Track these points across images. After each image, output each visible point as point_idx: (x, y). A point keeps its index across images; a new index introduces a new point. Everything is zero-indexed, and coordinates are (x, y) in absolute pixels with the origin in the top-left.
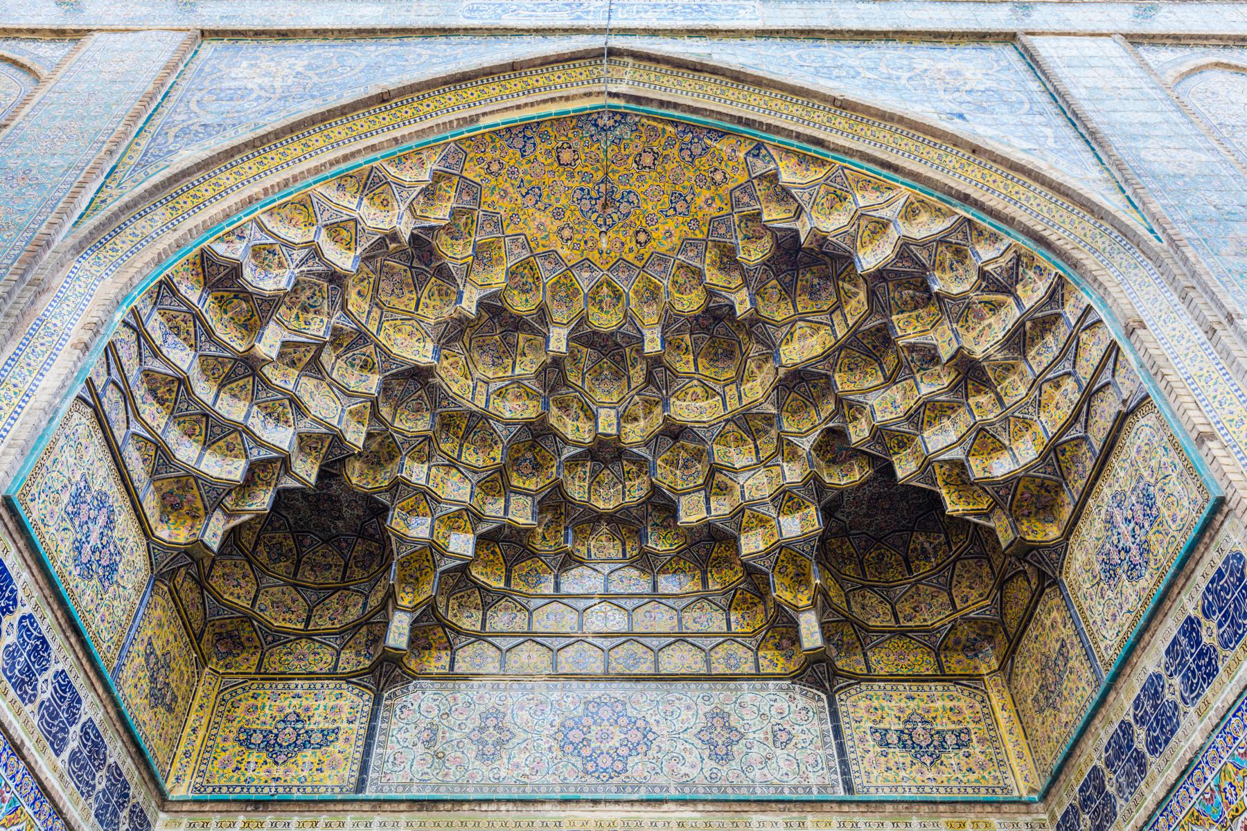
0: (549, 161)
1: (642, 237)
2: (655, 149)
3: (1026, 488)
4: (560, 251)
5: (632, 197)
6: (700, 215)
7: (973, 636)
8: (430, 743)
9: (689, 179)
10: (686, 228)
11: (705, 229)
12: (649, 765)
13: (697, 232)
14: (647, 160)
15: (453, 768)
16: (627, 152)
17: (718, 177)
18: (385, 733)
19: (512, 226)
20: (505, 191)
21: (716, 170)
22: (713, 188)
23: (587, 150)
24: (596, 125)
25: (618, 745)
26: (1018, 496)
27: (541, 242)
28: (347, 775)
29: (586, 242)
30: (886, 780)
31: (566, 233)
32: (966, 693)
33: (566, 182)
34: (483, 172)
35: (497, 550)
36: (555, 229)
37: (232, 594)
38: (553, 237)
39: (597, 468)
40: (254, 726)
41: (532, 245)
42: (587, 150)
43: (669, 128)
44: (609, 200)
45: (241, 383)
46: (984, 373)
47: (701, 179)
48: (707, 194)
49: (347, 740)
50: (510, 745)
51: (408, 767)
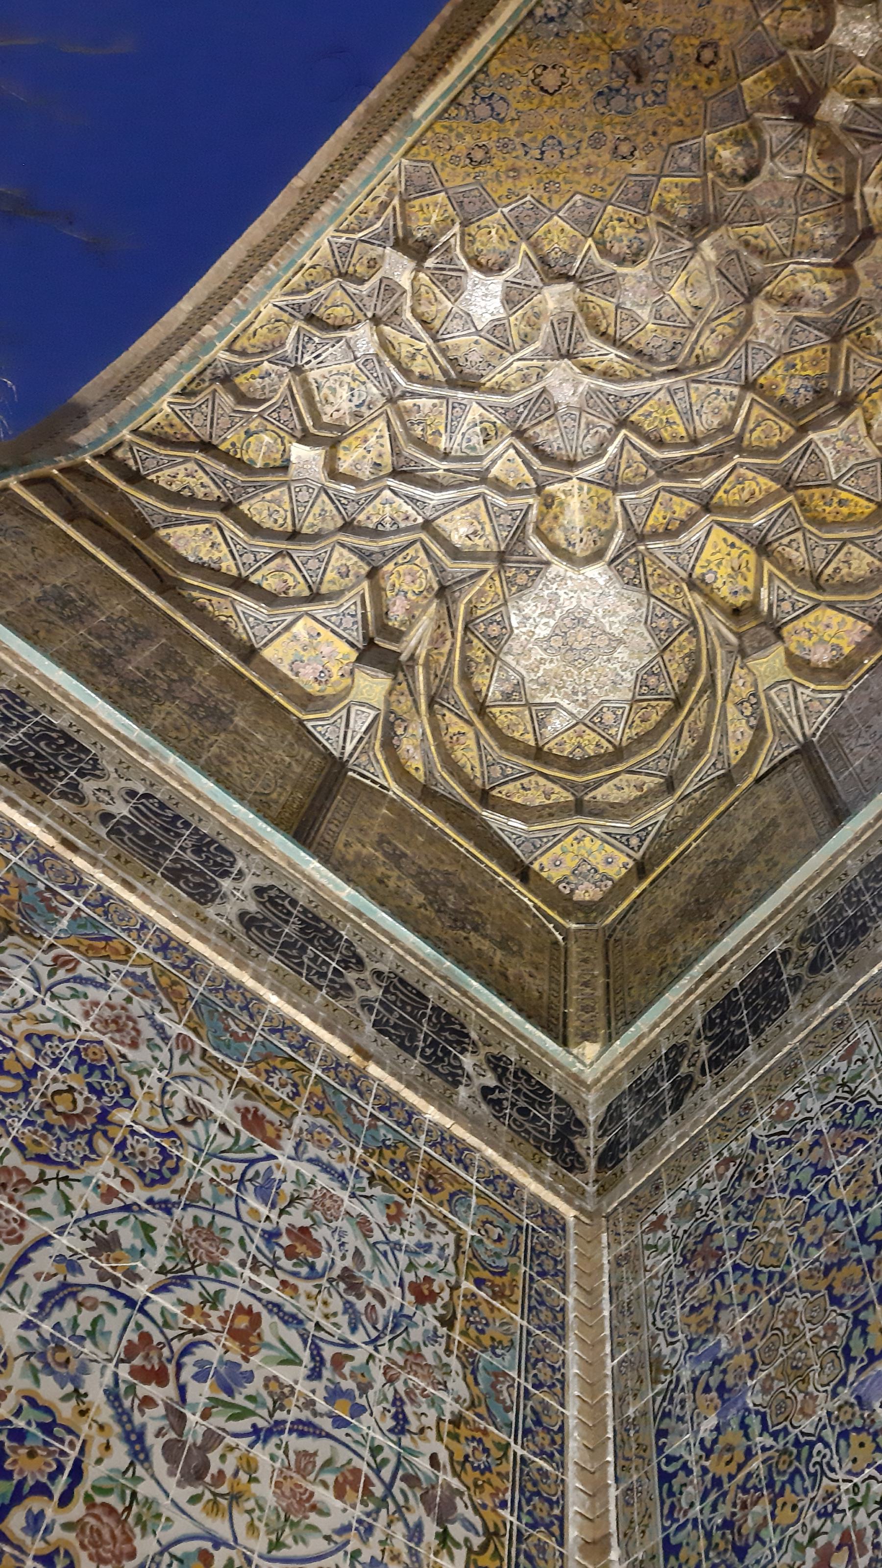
0: (536, 101)
4: (634, 170)
19: (555, 198)
20: (514, 169)
27: (604, 185)
31: (624, 149)
33: (576, 105)
34: (469, 169)
36: (607, 157)
38: (614, 166)
41: (597, 194)
45: (316, 510)
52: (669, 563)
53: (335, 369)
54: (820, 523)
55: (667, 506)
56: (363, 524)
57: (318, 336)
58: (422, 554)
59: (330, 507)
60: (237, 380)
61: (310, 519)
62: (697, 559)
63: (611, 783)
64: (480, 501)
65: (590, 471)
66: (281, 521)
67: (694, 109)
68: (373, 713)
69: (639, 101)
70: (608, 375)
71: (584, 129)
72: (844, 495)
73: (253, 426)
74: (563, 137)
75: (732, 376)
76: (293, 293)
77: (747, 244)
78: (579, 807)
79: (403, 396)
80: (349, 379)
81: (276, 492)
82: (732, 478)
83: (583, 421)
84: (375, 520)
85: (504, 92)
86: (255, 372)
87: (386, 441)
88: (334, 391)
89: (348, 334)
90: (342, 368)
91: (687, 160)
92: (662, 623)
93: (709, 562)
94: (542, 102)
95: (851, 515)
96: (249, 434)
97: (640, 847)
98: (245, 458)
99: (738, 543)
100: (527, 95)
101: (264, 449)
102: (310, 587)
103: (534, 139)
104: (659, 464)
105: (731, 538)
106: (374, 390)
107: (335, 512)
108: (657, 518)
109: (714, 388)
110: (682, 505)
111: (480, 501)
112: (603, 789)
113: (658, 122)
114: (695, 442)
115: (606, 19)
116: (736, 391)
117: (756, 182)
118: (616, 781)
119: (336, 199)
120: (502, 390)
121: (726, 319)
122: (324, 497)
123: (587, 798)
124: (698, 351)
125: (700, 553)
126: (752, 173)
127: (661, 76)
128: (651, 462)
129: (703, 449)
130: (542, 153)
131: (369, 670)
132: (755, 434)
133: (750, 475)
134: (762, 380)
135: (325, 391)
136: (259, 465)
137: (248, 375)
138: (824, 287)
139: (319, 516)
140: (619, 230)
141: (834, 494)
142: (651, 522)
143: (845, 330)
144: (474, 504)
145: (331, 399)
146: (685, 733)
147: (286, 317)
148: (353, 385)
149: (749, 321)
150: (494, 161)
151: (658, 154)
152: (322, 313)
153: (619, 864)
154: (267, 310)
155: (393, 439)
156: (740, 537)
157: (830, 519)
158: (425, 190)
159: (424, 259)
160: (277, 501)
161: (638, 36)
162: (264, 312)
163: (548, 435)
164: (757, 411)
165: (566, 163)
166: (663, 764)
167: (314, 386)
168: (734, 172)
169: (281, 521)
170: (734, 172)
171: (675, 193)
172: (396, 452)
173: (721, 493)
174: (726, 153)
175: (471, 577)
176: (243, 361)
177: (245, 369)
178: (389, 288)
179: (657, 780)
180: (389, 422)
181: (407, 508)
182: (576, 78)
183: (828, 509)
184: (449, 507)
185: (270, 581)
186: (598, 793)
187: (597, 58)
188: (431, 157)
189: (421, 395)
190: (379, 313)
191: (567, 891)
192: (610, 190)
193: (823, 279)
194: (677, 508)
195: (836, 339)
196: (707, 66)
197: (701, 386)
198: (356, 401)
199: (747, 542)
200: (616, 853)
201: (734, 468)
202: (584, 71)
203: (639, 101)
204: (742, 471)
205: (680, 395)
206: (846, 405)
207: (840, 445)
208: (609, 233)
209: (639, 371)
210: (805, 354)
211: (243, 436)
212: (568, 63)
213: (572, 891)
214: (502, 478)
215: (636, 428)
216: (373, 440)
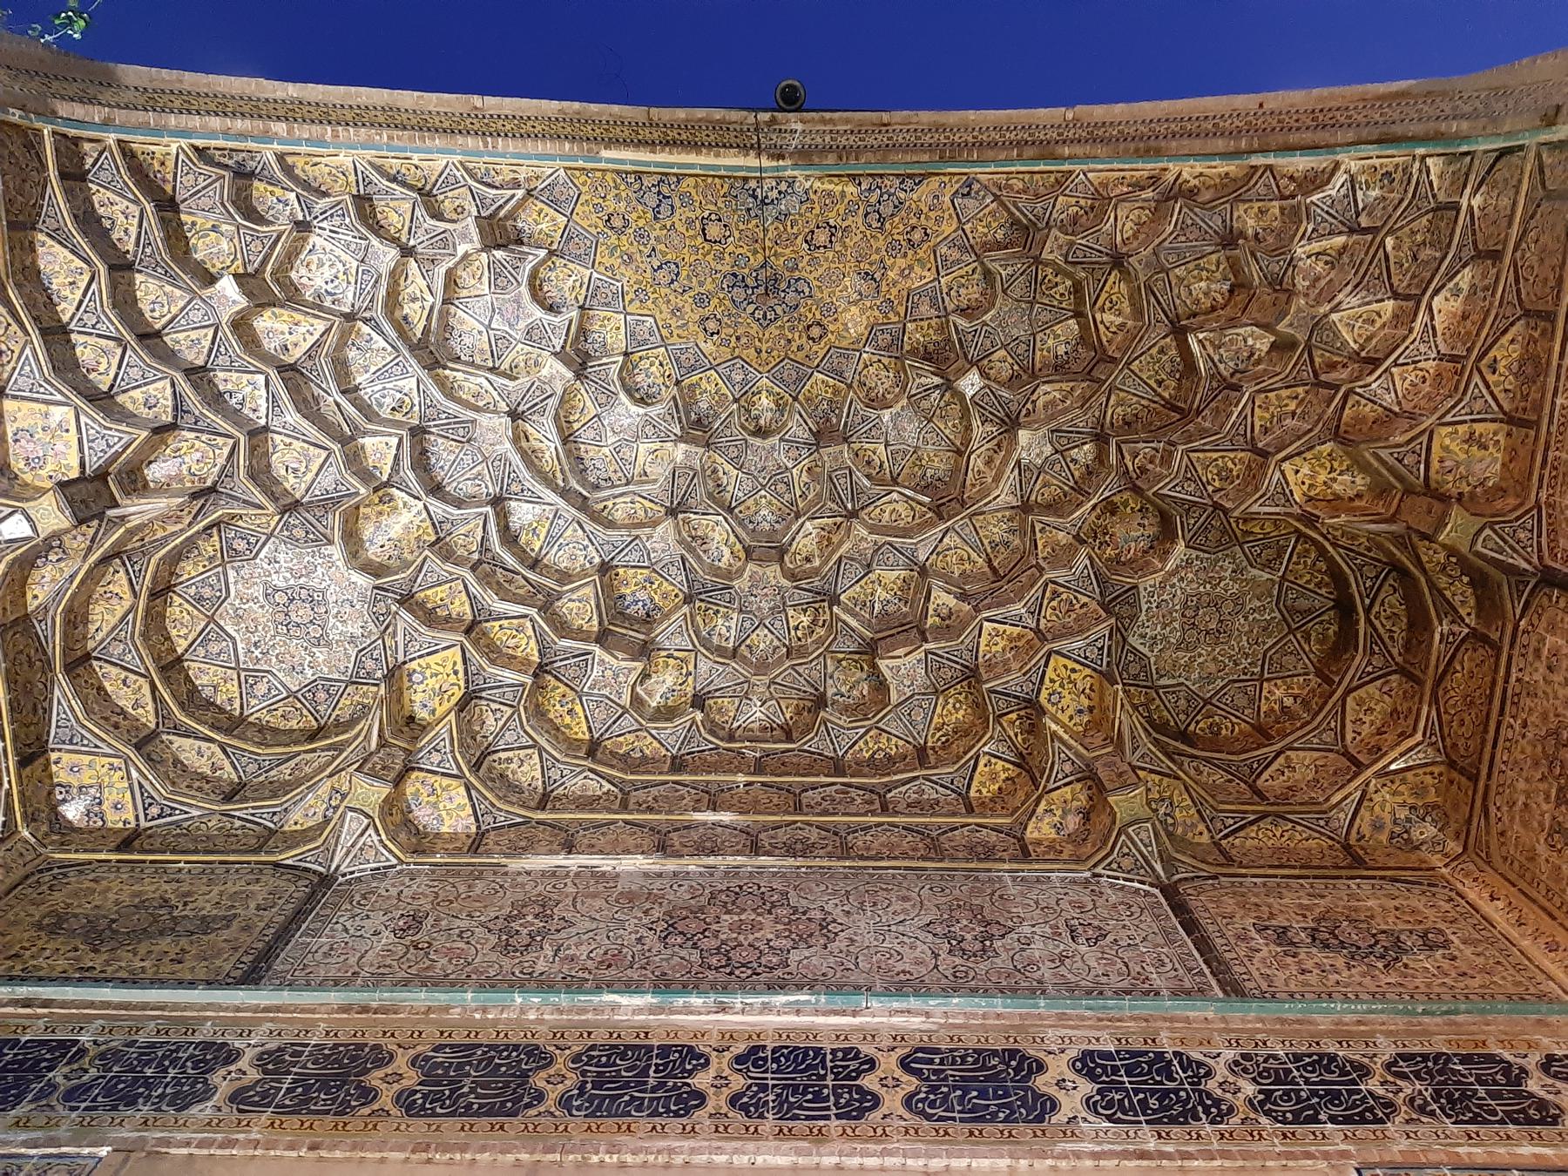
0: (691, 233)
1: (815, 332)
2: (832, 222)
3: (1446, 449)
4: (702, 345)
5: (801, 285)
6: (894, 291)
7: (1402, 814)
8: (401, 933)
9: (878, 250)
10: (877, 313)
11: (902, 310)
12: (832, 959)
13: (891, 315)
14: (822, 237)
15: (444, 961)
16: (795, 230)
17: (917, 236)
18: (325, 920)
20: (630, 257)
21: (913, 228)
22: (910, 253)
23: (742, 227)
24: (755, 197)
25: (770, 936)
26: (1435, 465)
28: (228, 967)
29: (738, 338)
30: (1305, 984)
31: (712, 325)
32: (1417, 892)
33: (713, 264)
35: (578, 708)
37: (106, 719)
38: (693, 328)
39: (747, 624)
40: (77, 911)
42: (742, 227)
43: (851, 189)
44: (771, 286)
46: (1337, 334)
47: (893, 248)
48: (901, 262)
49: (244, 929)
50: (563, 934)
51: (353, 960)
52: (400, 638)
53: (338, 252)
54: (539, 713)
55: (452, 594)
56: (216, 381)
57: (352, 218)
58: (226, 451)
59: (207, 343)
60: (256, 183)
61: (181, 336)
62: (421, 656)
63: (198, 743)
64: (324, 454)
65: (438, 508)
66: (156, 314)
67: (775, 353)
68: (28, 532)
69: (751, 308)
70: (530, 458)
71: (701, 284)
72: (578, 708)
73: (224, 227)
74: (684, 273)
75: (606, 547)
76: (379, 169)
77: (715, 471)
78: (145, 742)
79: (366, 321)
80: (342, 269)
81: (178, 293)
82: (515, 621)
83: (479, 468)
84: (229, 387)
85: (677, 203)
86: (278, 191)
87: (311, 340)
88: (321, 264)
89: (375, 241)
90: (344, 257)
91: (739, 378)
92: (370, 664)
93: (429, 666)
94: (694, 237)
95: (568, 726)
96: (214, 228)
97: (153, 819)
98: (193, 241)
99: (461, 674)
100: (690, 223)
101: (214, 250)
102: (112, 386)
103: (664, 254)
104: (489, 555)
105: (460, 667)
106: (350, 295)
107: (206, 351)
108: (434, 596)
109: (586, 542)
110: (462, 604)
111: (324, 454)
112: (187, 742)
113: (747, 334)
114: (534, 564)
115: (785, 236)
116: (597, 560)
117: (757, 442)
118: (204, 745)
119: (486, 144)
120: (449, 390)
121: (648, 504)
122: (211, 332)
123: (164, 737)
124: (610, 503)
125: (429, 654)
126: (761, 432)
127: (779, 310)
128: (484, 546)
129: (530, 575)
130: (660, 267)
131: (61, 498)
132: (570, 604)
133: (530, 632)
134: (621, 571)
135: (314, 258)
136: (198, 256)
137: (270, 188)
138: (726, 552)
139: (191, 344)
140: (653, 369)
141: (573, 701)
142: (429, 592)
143: (703, 597)
144: (318, 450)
145: (313, 267)
146: (292, 763)
147: (352, 178)
148: (340, 275)
149: (654, 524)
150: (623, 238)
151: (726, 353)
152: (380, 205)
153: (122, 814)
154: (344, 159)
155: (317, 344)
156: (466, 673)
157: (551, 716)
158: (554, 203)
159: (498, 247)
160: (171, 300)
161: (792, 270)
162: (341, 157)
163: (443, 452)
164: (589, 590)
165: (668, 291)
166: (252, 768)
167: (309, 247)
168: (757, 418)
169: (156, 314)
170: (757, 418)
171: (711, 388)
172: (309, 354)
173: (496, 624)
174: (765, 402)
175: (245, 501)
176: (279, 174)
177: (272, 181)
178: (445, 241)
179: (234, 776)
180: (328, 331)
181: (262, 403)
182: (731, 249)
183: (558, 707)
184: (295, 433)
185: (87, 351)
186: (178, 741)
187: (755, 252)
188: (584, 189)
189: (382, 333)
190: (419, 249)
191: (60, 797)
192: (675, 339)
193: (731, 548)
194: (457, 602)
195: (688, 600)
196: (809, 338)
197: (580, 532)
198: (330, 287)
199: (467, 682)
200: (130, 806)
201: (525, 616)
202: (740, 251)
203: (751, 308)
204: (529, 624)
205: (561, 522)
206: (645, 651)
207: (609, 673)
208: (645, 364)
209: (559, 474)
210: (665, 584)
211: (209, 226)
212: (736, 234)
213: (65, 801)
214: (369, 450)
215: (503, 517)
216: (302, 330)
